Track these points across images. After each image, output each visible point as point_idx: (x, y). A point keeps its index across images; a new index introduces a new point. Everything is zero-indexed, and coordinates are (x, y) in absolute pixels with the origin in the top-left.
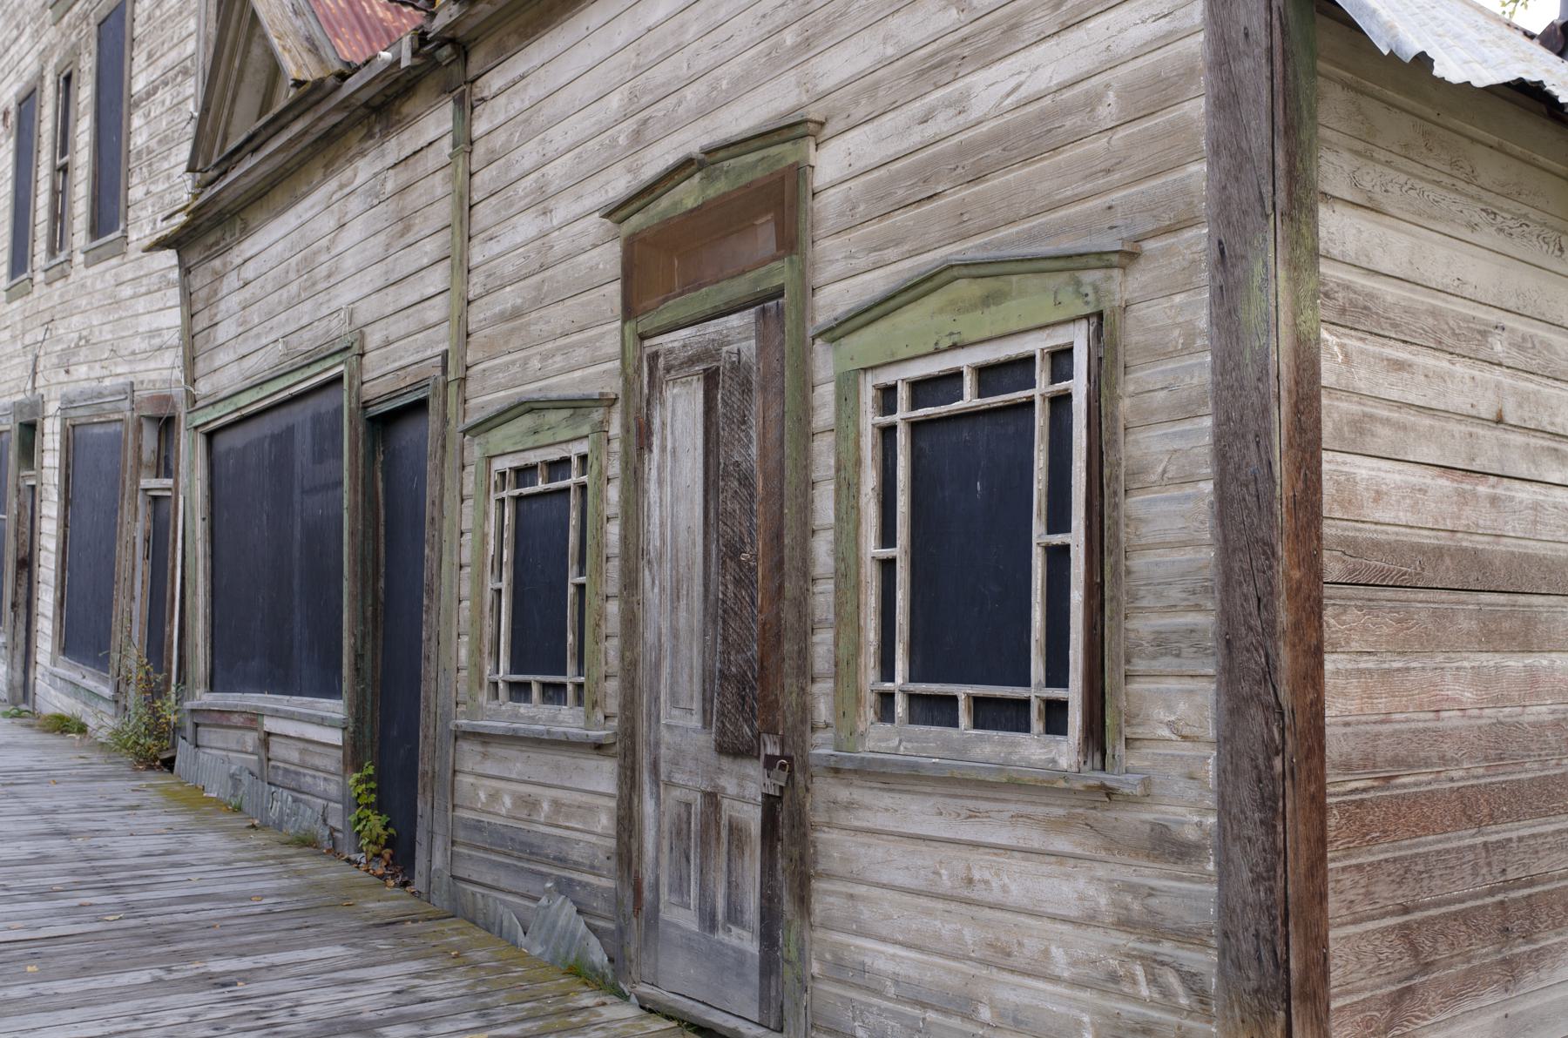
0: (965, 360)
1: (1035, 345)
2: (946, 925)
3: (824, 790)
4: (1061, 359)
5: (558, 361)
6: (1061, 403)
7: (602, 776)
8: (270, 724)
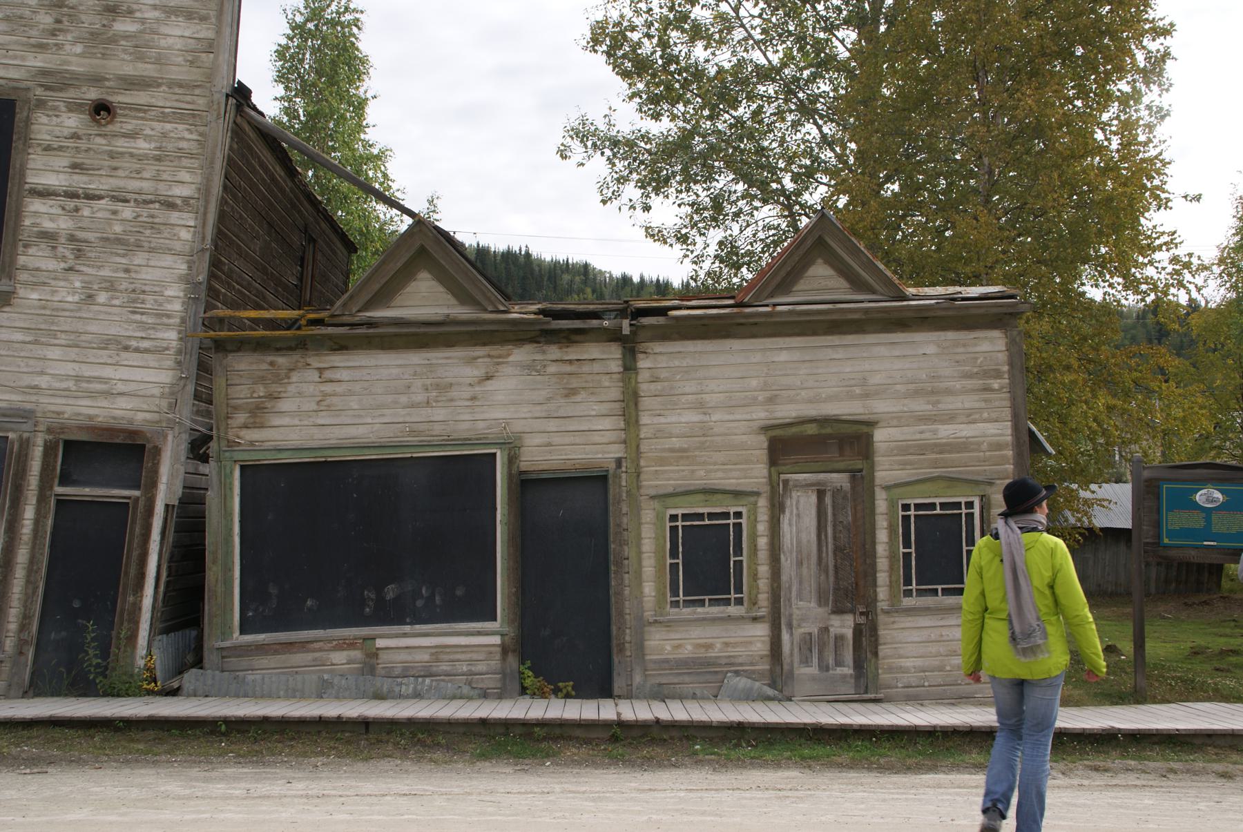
0: (937, 501)
1: (963, 500)
2: (933, 649)
3: (882, 619)
4: (970, 505)
5: (720, 474)
6: (970, 516)
7: (761, 631)
8: (380, 643)
